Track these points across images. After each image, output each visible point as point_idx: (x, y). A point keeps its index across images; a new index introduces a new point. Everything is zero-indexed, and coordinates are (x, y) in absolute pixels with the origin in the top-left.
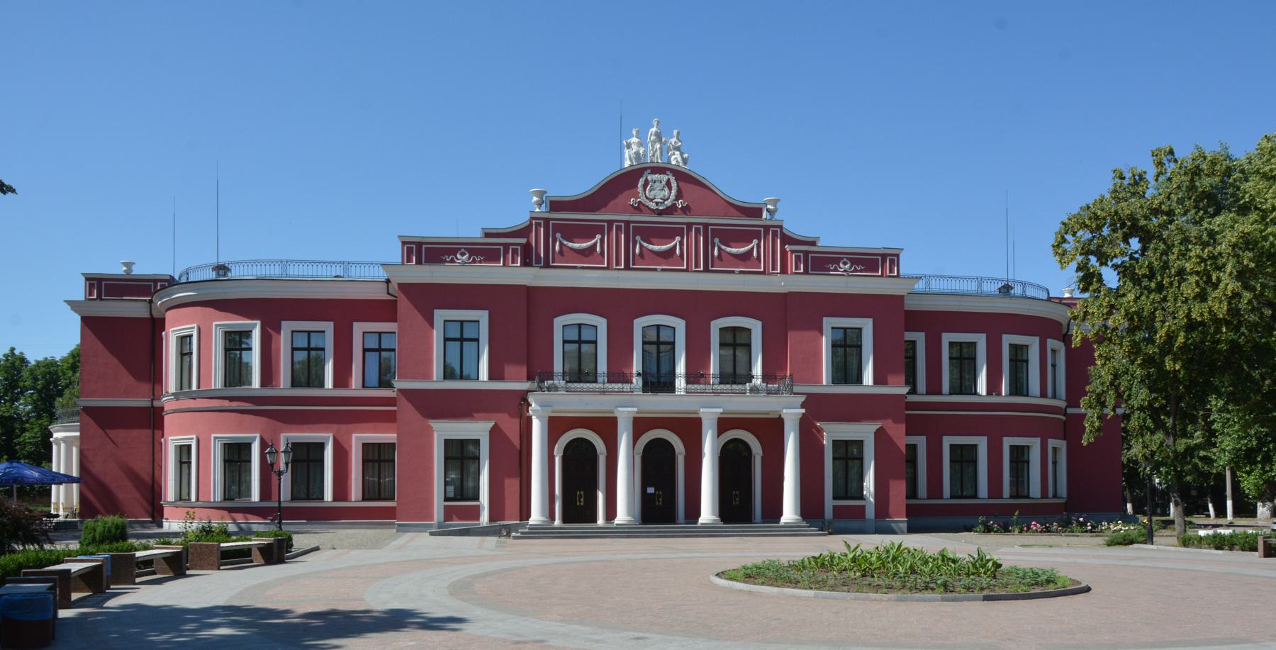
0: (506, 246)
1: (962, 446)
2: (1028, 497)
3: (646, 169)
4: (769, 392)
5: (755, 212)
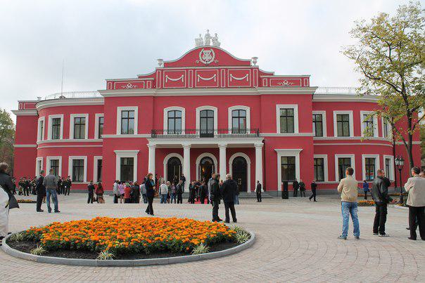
0: (146, 81)
4: (252, 137)
5: (248, 63)
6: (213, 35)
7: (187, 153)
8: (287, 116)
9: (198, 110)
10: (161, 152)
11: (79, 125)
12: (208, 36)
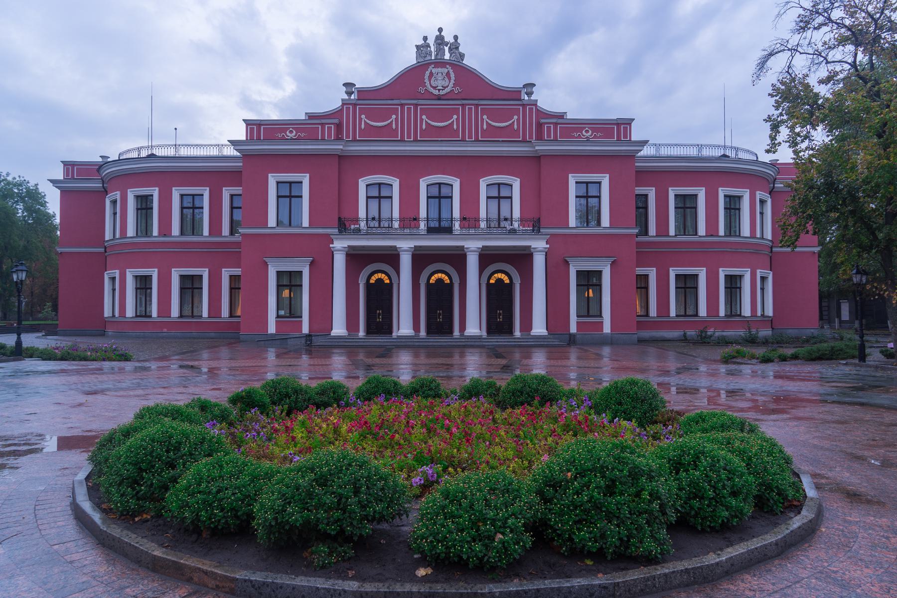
0: (323, 125)
1: (685, 276)
2: (740, 315)
3: (430, 64)
4: (524, 233)
5: (513, 95)
6: (449, 38)
7: (406, 262)
8: (588, 195)
9: (423, 184)
10: (357, 259)
11: (191, 207)
12: (440, 40)
